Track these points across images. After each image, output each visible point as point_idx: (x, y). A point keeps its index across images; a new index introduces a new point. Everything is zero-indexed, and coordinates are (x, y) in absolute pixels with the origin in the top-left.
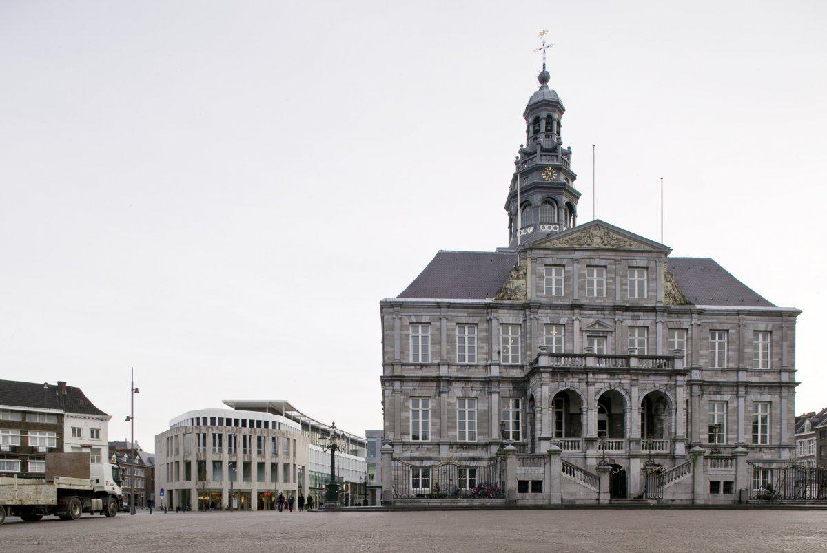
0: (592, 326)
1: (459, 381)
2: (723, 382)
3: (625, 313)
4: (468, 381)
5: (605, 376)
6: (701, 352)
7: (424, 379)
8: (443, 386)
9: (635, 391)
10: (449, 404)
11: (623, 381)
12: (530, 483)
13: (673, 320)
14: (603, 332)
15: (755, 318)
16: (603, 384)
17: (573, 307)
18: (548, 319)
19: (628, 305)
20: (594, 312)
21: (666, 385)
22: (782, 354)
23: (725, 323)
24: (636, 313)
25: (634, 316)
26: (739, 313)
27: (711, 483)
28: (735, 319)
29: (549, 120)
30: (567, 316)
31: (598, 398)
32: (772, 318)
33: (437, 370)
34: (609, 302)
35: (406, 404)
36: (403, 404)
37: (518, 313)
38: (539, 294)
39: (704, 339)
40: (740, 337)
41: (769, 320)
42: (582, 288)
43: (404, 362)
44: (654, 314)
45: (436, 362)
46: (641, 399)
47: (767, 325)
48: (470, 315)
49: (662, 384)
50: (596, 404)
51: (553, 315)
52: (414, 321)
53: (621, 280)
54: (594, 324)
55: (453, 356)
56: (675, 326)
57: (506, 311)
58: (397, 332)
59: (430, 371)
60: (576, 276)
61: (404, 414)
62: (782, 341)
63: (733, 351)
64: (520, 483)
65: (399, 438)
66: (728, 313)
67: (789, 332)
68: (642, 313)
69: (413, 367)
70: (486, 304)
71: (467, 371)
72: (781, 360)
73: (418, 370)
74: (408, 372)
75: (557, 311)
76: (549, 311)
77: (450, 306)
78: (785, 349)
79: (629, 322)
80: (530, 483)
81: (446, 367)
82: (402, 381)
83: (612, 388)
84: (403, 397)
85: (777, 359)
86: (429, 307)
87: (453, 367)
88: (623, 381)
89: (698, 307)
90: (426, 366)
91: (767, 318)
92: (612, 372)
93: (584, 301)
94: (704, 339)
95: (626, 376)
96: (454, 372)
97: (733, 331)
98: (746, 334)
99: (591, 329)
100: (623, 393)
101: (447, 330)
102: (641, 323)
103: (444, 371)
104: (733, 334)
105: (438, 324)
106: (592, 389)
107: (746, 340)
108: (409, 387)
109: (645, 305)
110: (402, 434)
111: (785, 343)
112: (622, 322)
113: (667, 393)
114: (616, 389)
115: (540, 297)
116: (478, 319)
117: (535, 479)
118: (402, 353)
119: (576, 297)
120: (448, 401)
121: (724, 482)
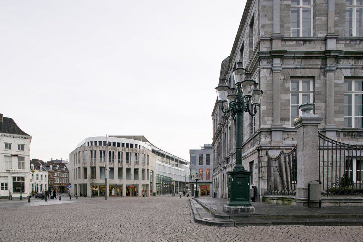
7: (308, 56)
10: (336, 85)
33: (323, 45)
35: (287, 85)
36: (283, 85)
43: (286, 36)
45: (321, 35)
55: (341, 29)
59: (315, 47)
65: (279, 124)
69: (294, 43)
71: (357, 46)
73: (300, 45)
74: (291, 47)
87: (341, 42)
90: (310, 41)
96: (342, 47)
103: (332, 45)
108: (290, 64)
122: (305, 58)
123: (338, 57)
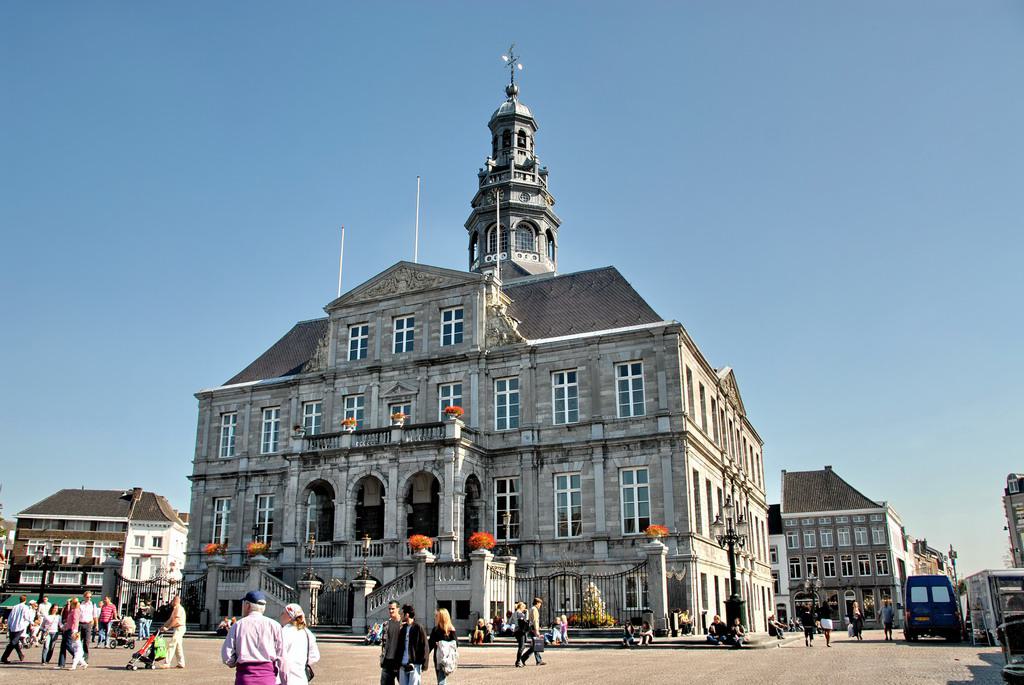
0: (394, 390)
1: (257, 476)
2: (570, 444)
3: (432, 368)
4: (267, 475)
5: (360, 458)
6: (539, 405)
7: (225, 477)
8: (242, 486)
9: (393, 473)
11: (381, 462)
12: (230, 603)
13: (496, 366)
14: (406, 396)
15: (614, 344)
16: (360, 465)
17: (371, 370)
18: (346, 389)
19: (436, 357)
20: (397, 373)
21: (434, 461)
22: (657, 391)
23: (571, 358)
24: (445, 366)
25: (442, 369)
26: (588, 342)
27: (438, 602)
28: (583, 353)
29: (508, 136)
30: (367, 382)
31: (351, 487)
32: (642, 340)
34: (414, 356)
37: (319, 387)
38: (339, 361)
39: (542, 385)
40: (594, 375)
41: (635, 344)
42: (387, 345)
44: (467, 363)
46: (403, 483)
47: (633, 353)
48: (273, 397)
49: (429, 461)
50: (349, 495)
51: (351, 384)
52: (223, 411)
53: (429, 327)
54: (396, 388)
56: (500, 374)
57: (307, 386)
58: (207, 425)
60: (379, 332)
61: (207, 519)
62: (656, 372)
63: (582, 396)
64: (224, 604)
66: (573, 345)
67: (667, 357)
68: (452, 365)
70: (286, 382)
72: (657, 399)
75: (356, 378)
76: (347, 379)
77: (254, 389)
78: (662, 381)
79: (437, 379)
80: (230, 603)
81: (246, 460)
82: (205, 480)
83: (368, 473)
84: (206, 499)
85: (652, 400)
86: (236, 393)
88: (381, 462)
89: (531, 343)
91: (633, 342)
92: (368, 452)
93: (387, 360)
94: (542, 385)
95: (386, 455)
96: (254, 465)
97: (584, 368)
98: (602, 370)
99: (394, 394)
100: (380, 477)
101: (251, 417)
102: (452, 377)
103: (243, 465)
104: (581, 372)
105: (243, 411)
106: (345, 474)
107: (602, 378)
108: (212, 486)
109: (459, 354)
110: (202, 542)
111: (661, 375)
112: (427, 380)
113: (436, 473)
114: (374, 474)
115: (340, 364)
116: (282, 399)
117: (236, 599)
118: (209, 448)
119: (377, 358)
120: (247, 500)
121: (457, 602)
122: (223, 478)
123: (249, 476)
